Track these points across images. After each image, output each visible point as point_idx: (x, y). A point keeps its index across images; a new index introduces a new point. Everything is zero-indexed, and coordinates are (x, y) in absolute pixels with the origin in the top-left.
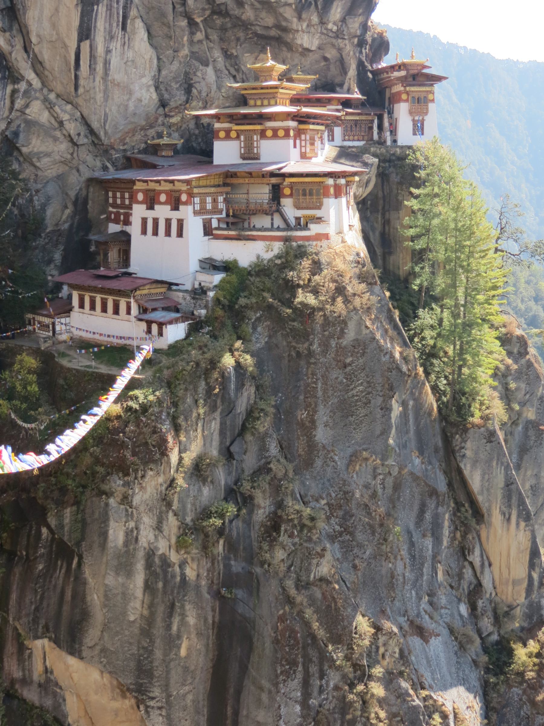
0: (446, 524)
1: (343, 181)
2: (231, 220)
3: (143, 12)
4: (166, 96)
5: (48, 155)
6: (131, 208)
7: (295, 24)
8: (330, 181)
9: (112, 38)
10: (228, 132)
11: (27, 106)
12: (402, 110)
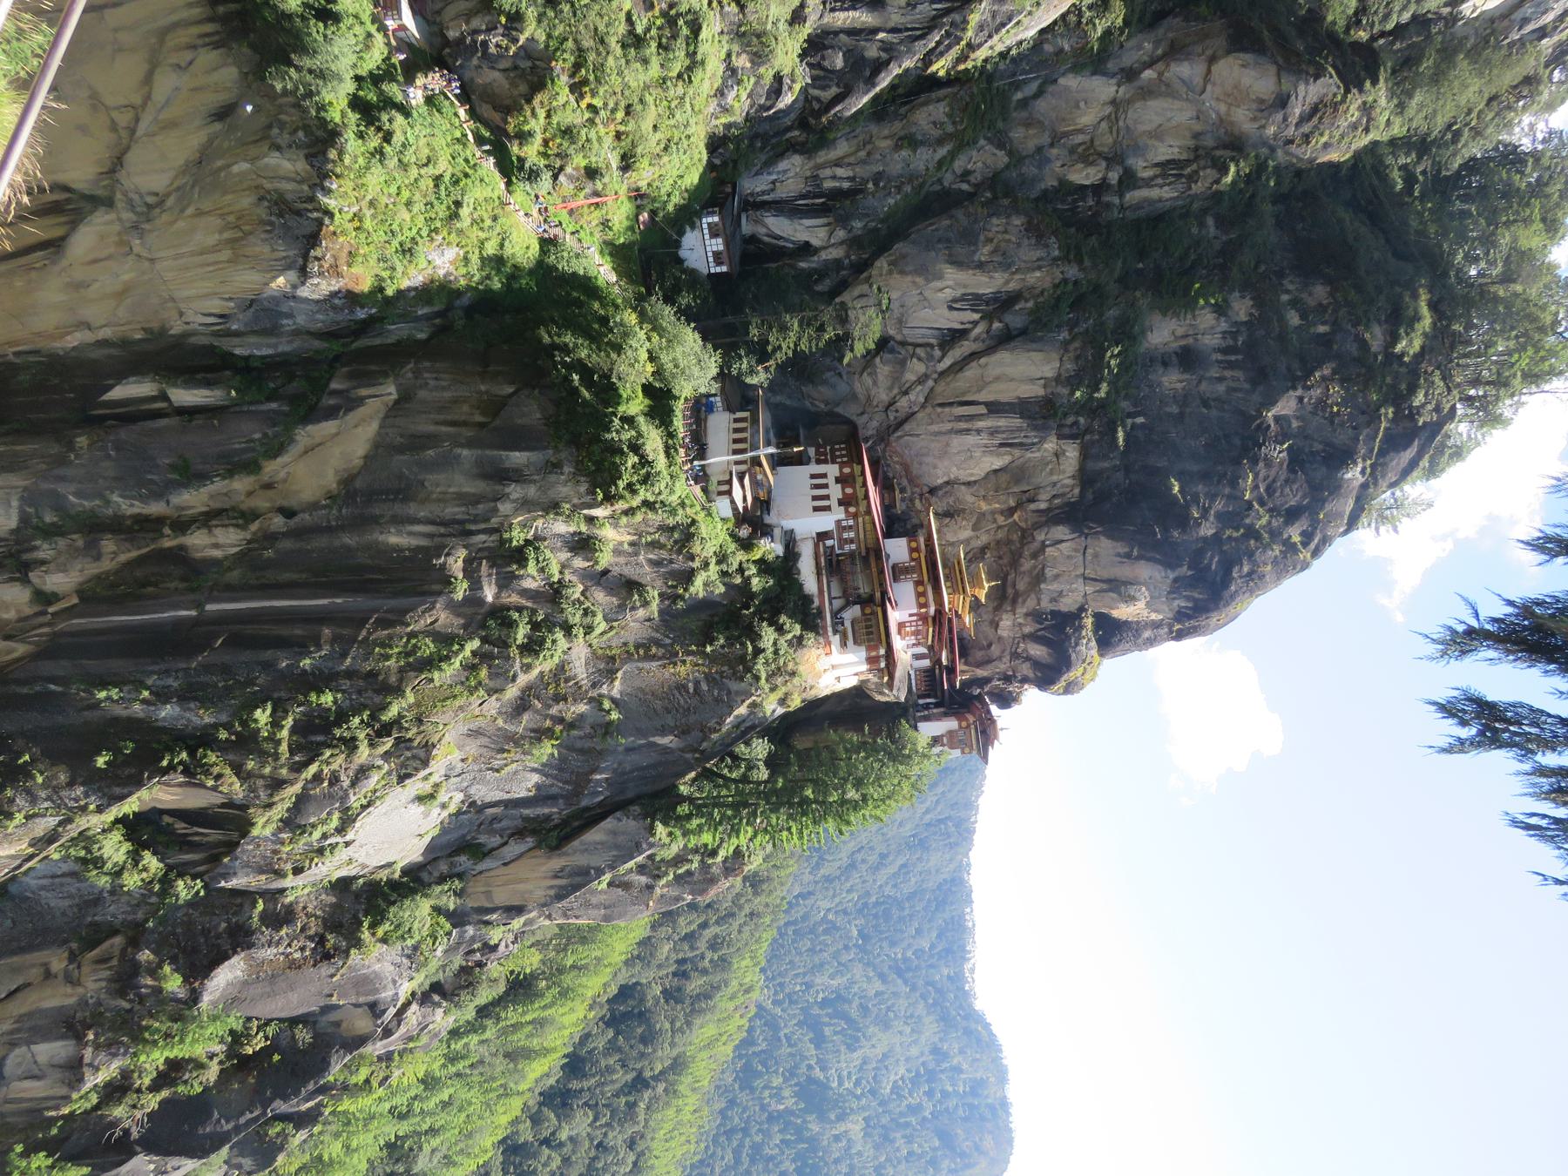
0: (546, 811)
1: (883, 665)
5: (875, 383)
6: (833, 462)
7: (1021, 610)
8: (882, 652)
9: (992, 434)
10: (917, 550)
11: (920, 359)
12: (951, 724)
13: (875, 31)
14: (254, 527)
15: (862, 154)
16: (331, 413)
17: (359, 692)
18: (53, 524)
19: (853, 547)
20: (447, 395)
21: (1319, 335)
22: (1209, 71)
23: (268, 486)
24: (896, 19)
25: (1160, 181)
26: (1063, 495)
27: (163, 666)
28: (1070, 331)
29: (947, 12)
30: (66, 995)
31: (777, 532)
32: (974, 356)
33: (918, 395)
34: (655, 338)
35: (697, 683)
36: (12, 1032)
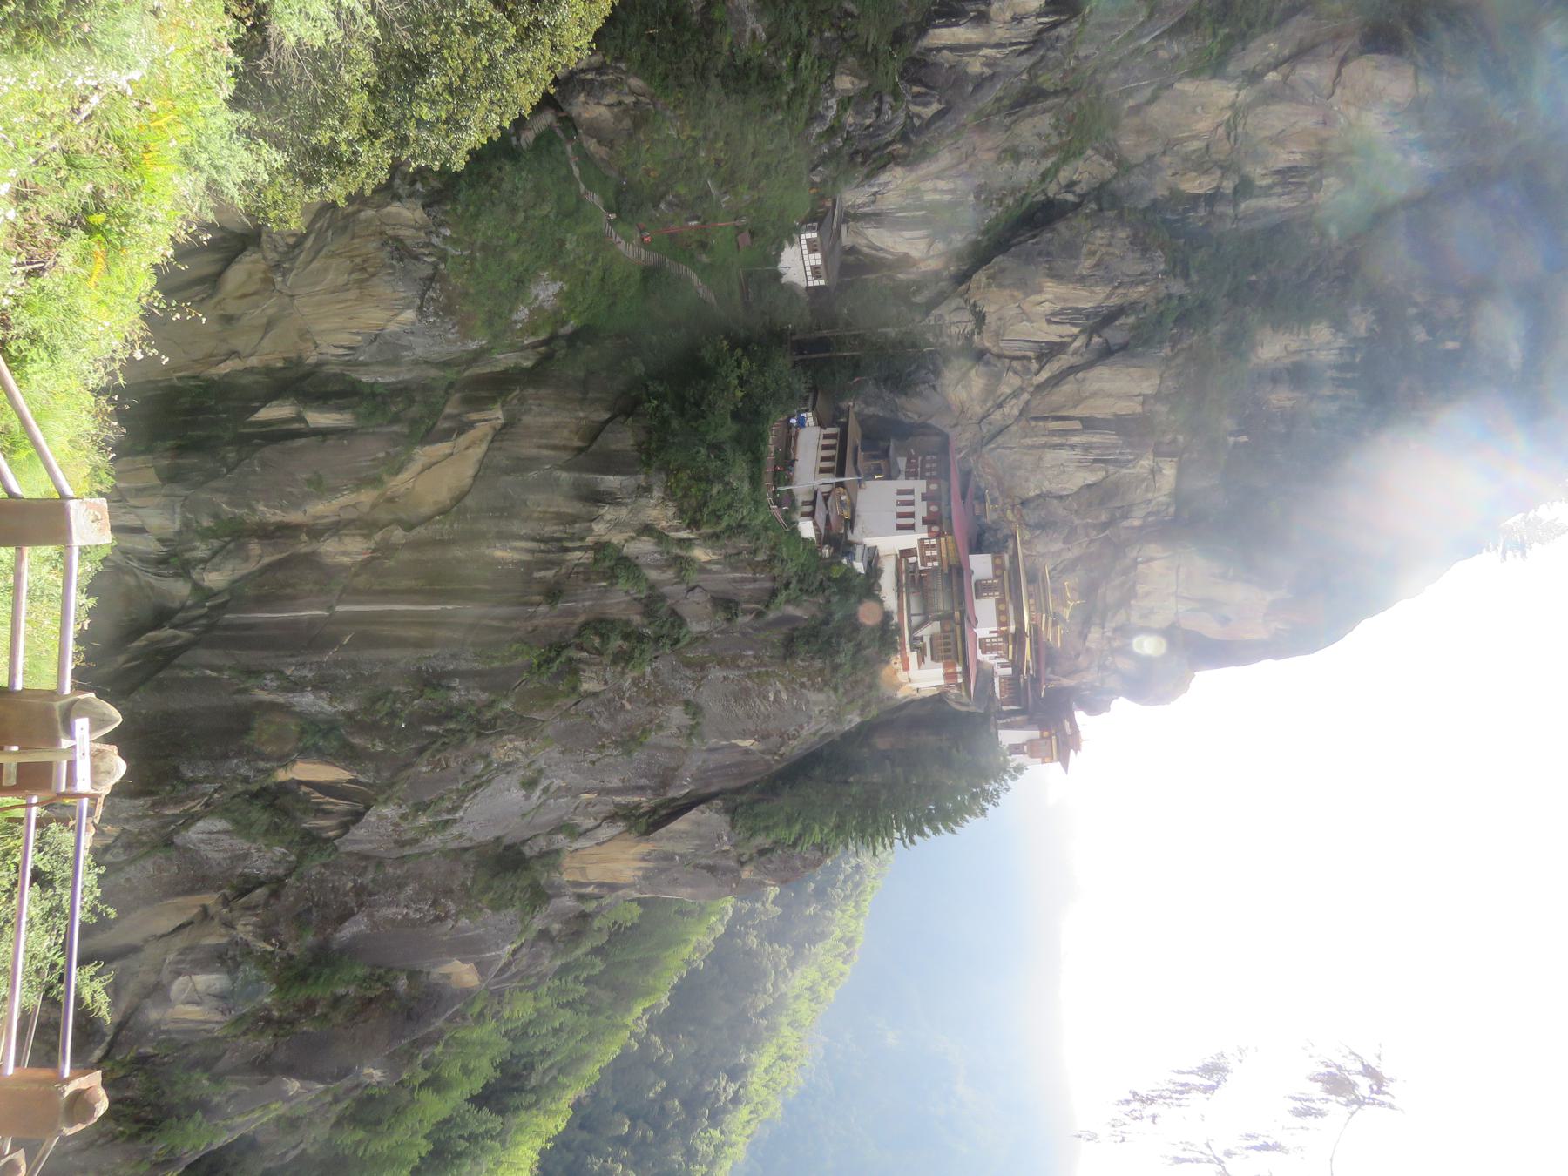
0: (636, 799)
1: (960, 680)
2: (917, 575)
3: (1112, 478)
4: (1032, 505)
7: (1110, 625)
8: (959, 669)
11: (1016, 372)
13: (979, 46)
14: (378, 537)
15: (964, 166)
16: (446, 436)
17: (467, 690)
18: (209, 529)
19: (936, 564)
20: (549, 420)
21: (1448, 352)
22: (1339, 73)
23: (391, 500)
24: (1000, 33)
25: (1278, 190)
26: (1158, 513)
27: (299, 659)
28: (1173, 347)
29: (1054, 25)
30: (222, 936)
31: (859, 551)
32: (1072, 370)
33: (1013, 409)
34: (745, 362)
35: (777, 693)
36: (178, 962)
